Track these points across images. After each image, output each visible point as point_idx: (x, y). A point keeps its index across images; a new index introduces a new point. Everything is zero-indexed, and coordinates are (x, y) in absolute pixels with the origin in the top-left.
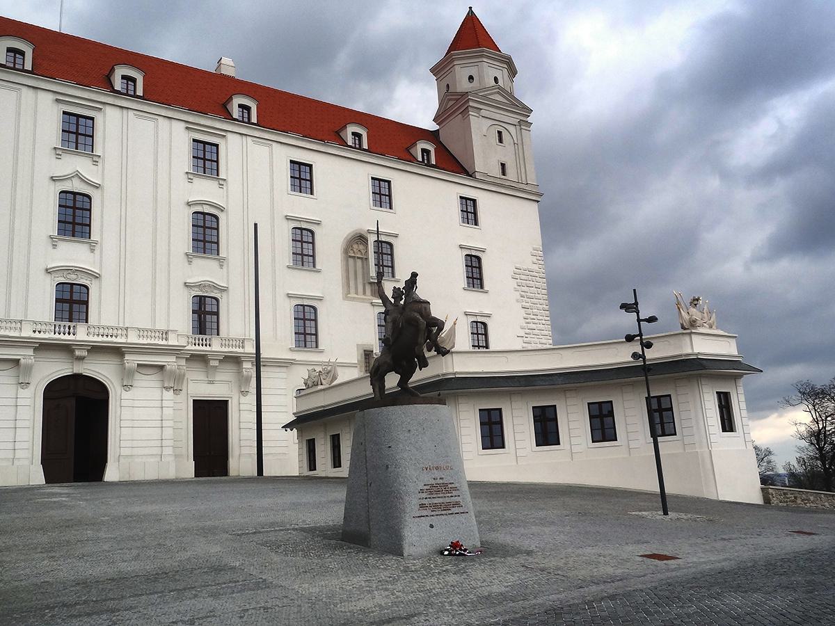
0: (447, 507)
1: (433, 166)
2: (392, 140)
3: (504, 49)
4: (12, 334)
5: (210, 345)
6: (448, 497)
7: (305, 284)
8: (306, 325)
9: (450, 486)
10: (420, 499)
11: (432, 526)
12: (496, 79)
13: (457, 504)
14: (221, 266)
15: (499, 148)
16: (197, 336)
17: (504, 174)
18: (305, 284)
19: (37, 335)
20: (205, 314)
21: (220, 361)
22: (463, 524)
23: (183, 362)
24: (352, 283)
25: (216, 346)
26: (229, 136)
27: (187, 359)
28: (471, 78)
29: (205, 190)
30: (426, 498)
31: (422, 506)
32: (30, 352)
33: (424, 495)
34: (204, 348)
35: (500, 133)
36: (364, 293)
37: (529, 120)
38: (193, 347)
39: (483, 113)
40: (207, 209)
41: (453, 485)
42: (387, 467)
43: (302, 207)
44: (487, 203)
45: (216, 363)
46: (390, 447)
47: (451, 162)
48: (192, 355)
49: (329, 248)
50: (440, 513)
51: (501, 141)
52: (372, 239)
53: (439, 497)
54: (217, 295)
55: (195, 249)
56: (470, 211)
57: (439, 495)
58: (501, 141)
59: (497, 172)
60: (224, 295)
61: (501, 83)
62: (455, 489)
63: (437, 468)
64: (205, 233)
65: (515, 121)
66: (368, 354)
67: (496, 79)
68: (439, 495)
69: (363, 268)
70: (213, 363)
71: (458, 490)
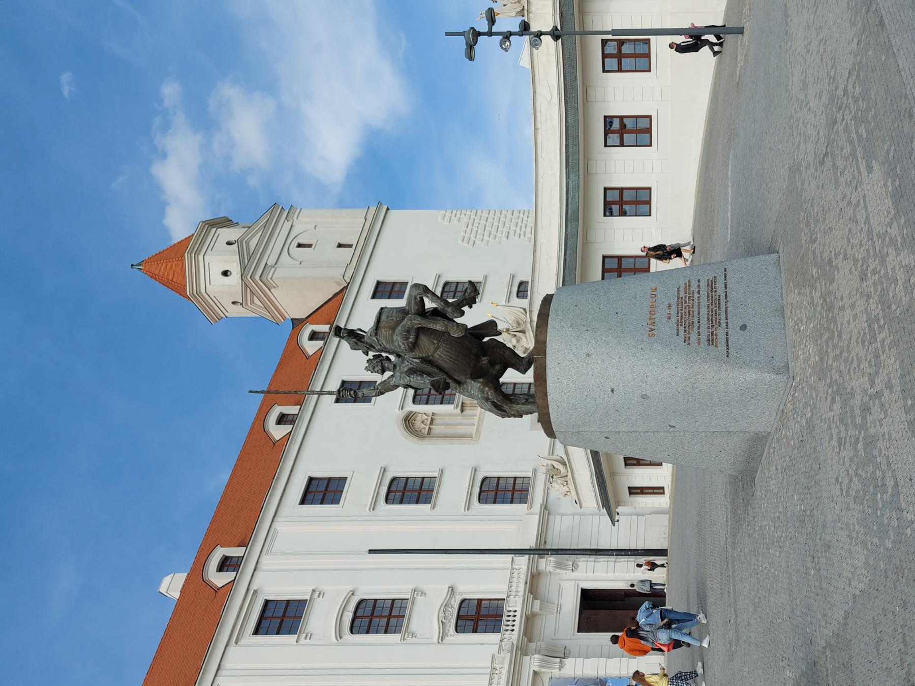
0: (715, 302)
5: (515, 611)
7: (454, 490)
9: (682, 294)
10: (699, 343)
11: (744, 327)
13: (712, 284)
16: (503, 628)
18: (454, 490)
20: (478, 616)
23: (532, 646)
25: (515, 605)
27: (530, 641)
30: (699, 333)
31: (711, 341)
33: (694, 337)
34: (518, 619)
35: (299, 245)
42: (644, 397)
46: (612, 391)
48: (525, 634)
51: (310, 246)
54: (458, 599)
58: (310, 246)
62: (688, 285)
63: (652, 313)
70: (536, 608)
71: (689, 281)
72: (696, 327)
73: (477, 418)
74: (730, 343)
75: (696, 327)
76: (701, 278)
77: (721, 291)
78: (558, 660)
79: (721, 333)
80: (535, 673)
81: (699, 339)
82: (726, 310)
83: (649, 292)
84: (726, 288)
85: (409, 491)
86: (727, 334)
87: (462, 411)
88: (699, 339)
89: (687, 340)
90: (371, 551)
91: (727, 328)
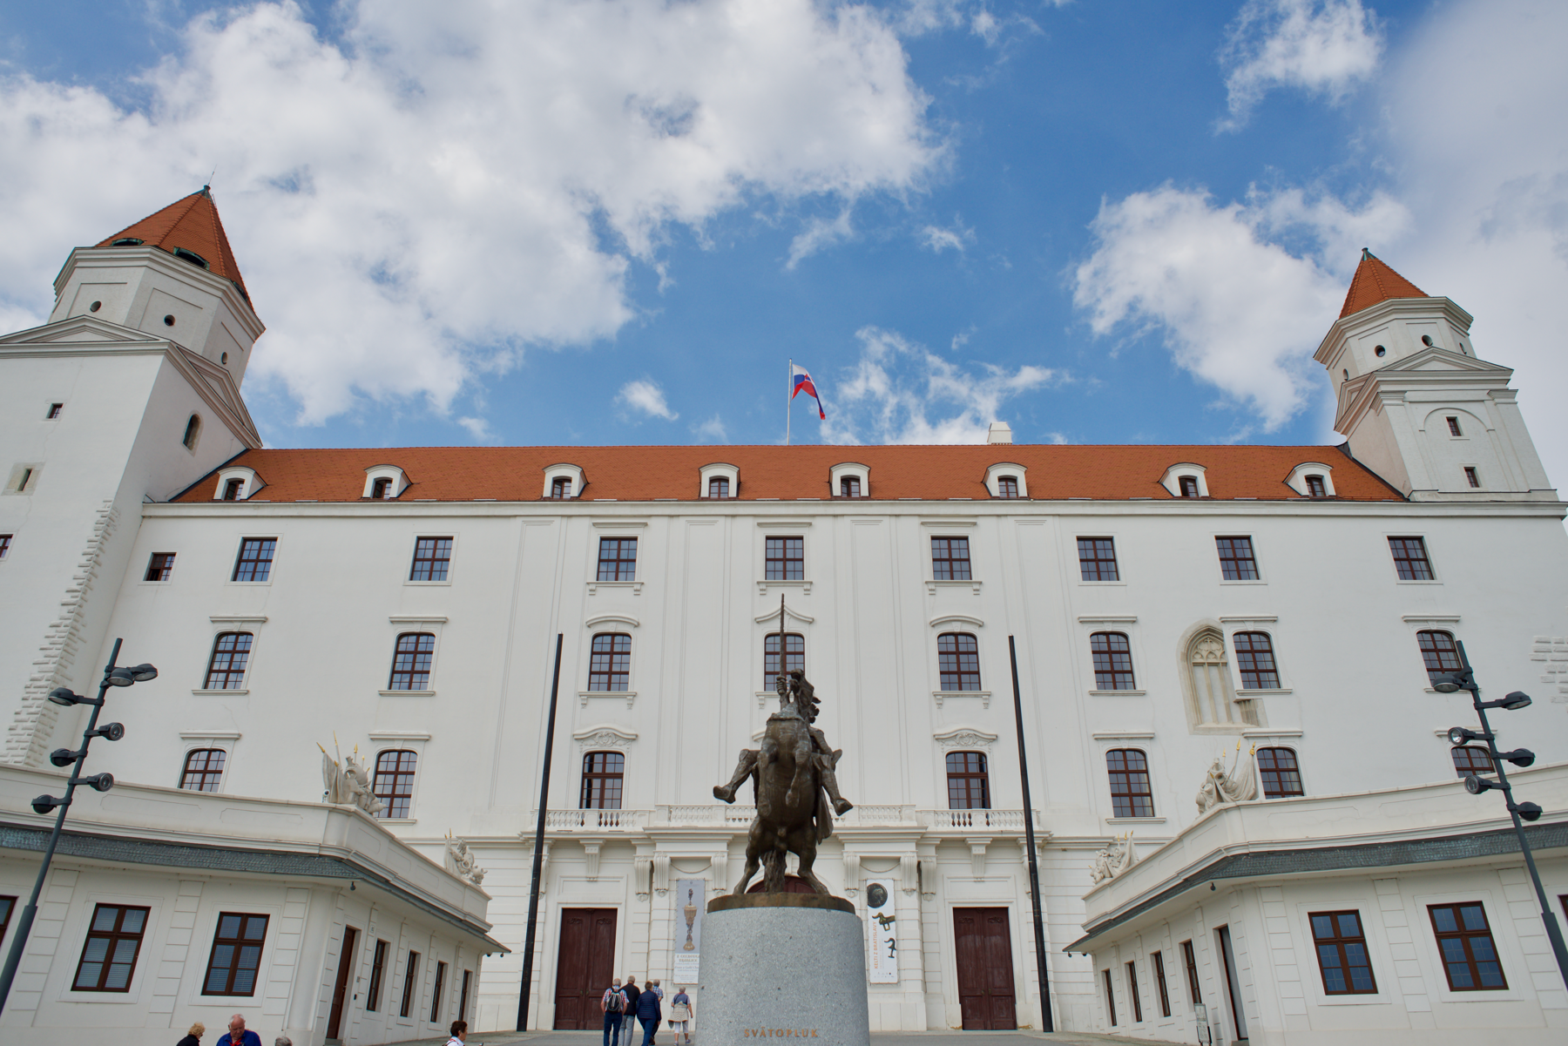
1: (1331, 498)
2: (1256, 471)
3: (1433, 289)
4: (701, 824)
7: (1121, 717)
8: (1130, 782)
12: (1426, 340)
14: (986, 705)
15: (1457, 443)
16: (956, 811)
17: (1474, 481)
18: (1121, 717)
19: (731, 824)
21: (988, 847)
23: (932, 851)
24: (1206, 705)
26: (979, 521)
27: (938, 848)
28: (1380, 350)
29: (954, 602)
32: (723, 847)
36: (1230, 717)
37: (1510, 386)
38: (951, 828)
39: (1410, 396)
40: (956, 628)
43: (1105, 601)
44: (1440, 538)
45: (982, 851)
47: (1364, 485)
48: (943, 840)
49: (1156, 657)
52: (1228, 632)
55: (945, 685)
56: (1411, 557)
59: (1463, 483)
60: (994, 746)
61: (1436, 342)
64: (959, 663)
65: (1483, 395)
67: (1426, 340)
69: (1222, 679)
73: (1230, 725)
78: (915, 885)
80: (898, 859)
85: (1112, 661)
87: (1238, 702)
90: (1011, 638)
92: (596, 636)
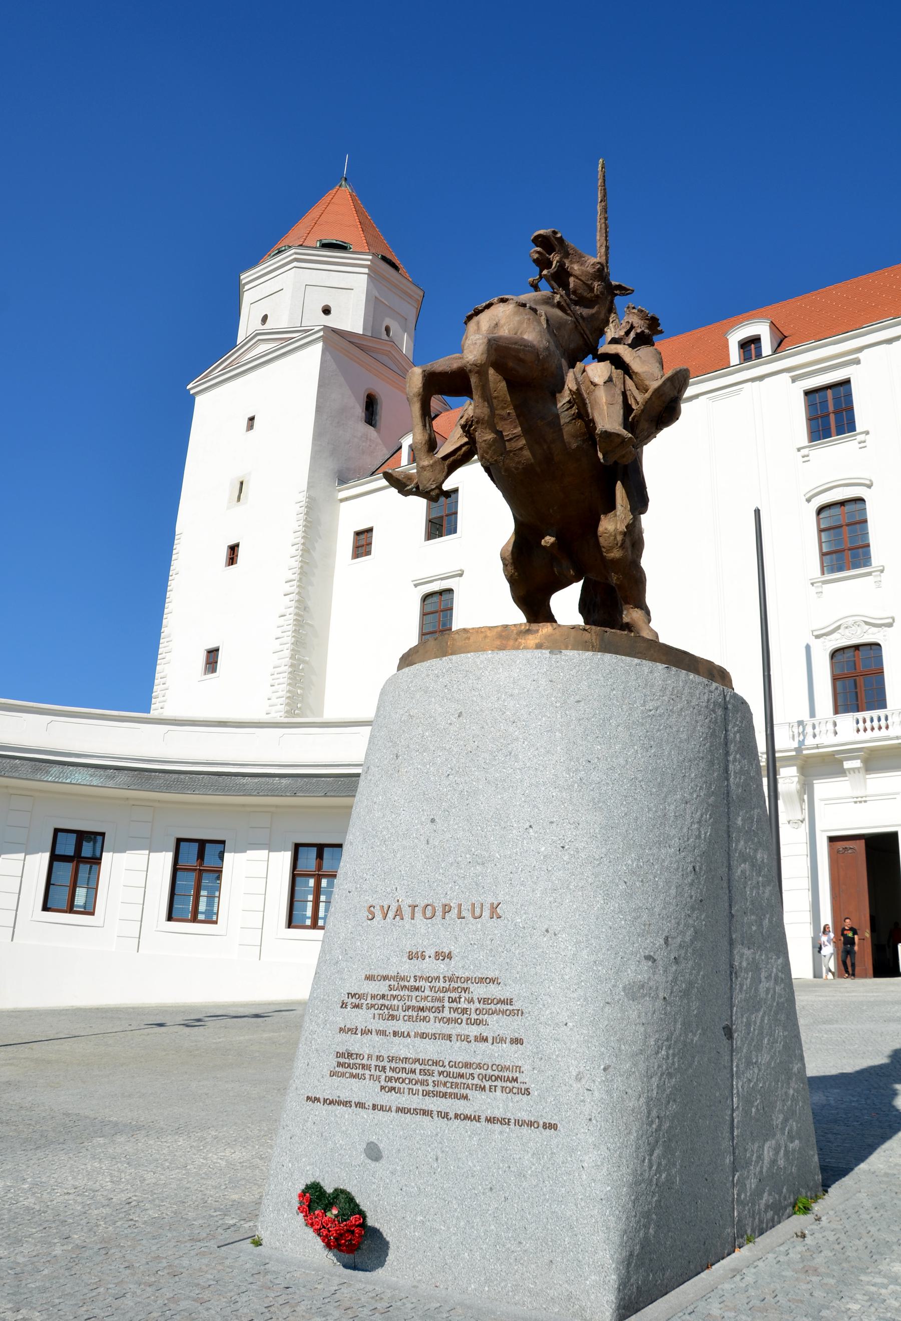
0: (455, 1081)
6: (466, 1038)
9: (479, 991)
22: (521, 1175)
30: (366, 1032)
31: (347, 1064)
33: (362, 1018)
41: (493, 991)
50: (416, 1102)
53: (423, 1036)
57: (423, 1027)
62: (504, 1006)
66: (320, 537)
68: (423, 1027)
71: (519, 1012)
72: (382, 1025)
74: (341, 1108)
75: (382, 1025)
76: (527, 1048)
77: (481, 1103)
79: (364, 1089)
81: (354, 1031)
82: (425, 1113)
83: (490, 899)
84: (489, 1120)
86: (360, 1105)
88: (354, 1031)
89: (355, 1000)
91: (374, 1107)
92: (820, 511)
